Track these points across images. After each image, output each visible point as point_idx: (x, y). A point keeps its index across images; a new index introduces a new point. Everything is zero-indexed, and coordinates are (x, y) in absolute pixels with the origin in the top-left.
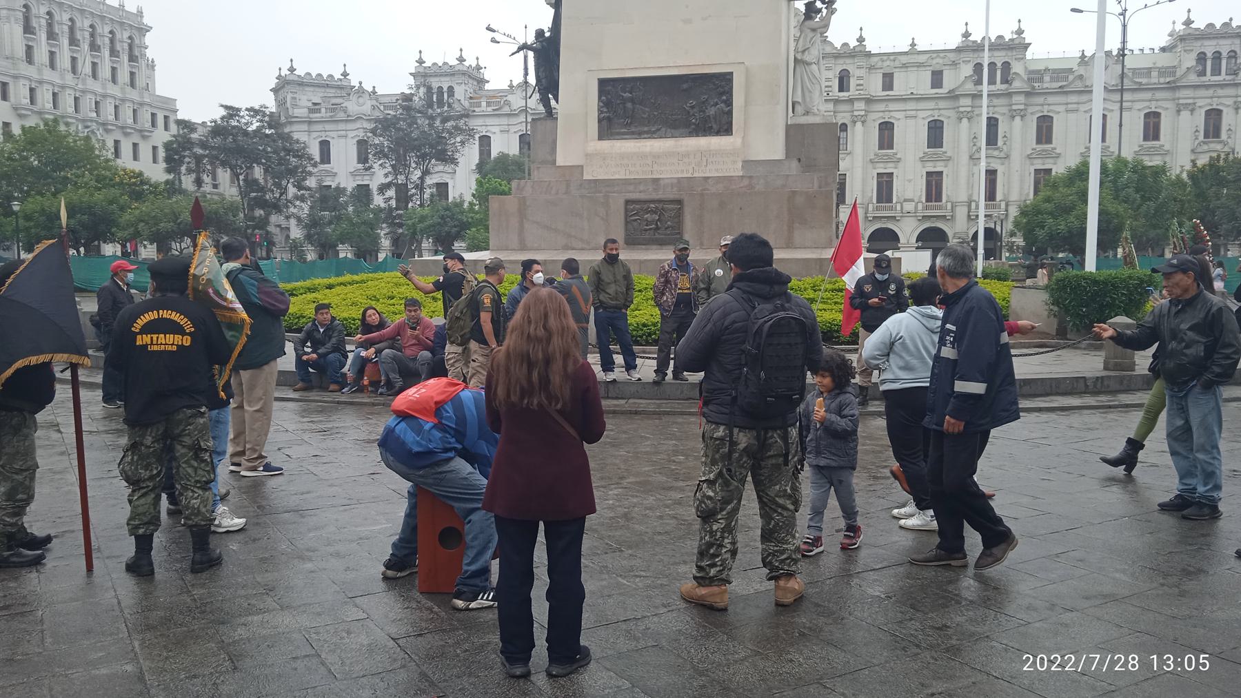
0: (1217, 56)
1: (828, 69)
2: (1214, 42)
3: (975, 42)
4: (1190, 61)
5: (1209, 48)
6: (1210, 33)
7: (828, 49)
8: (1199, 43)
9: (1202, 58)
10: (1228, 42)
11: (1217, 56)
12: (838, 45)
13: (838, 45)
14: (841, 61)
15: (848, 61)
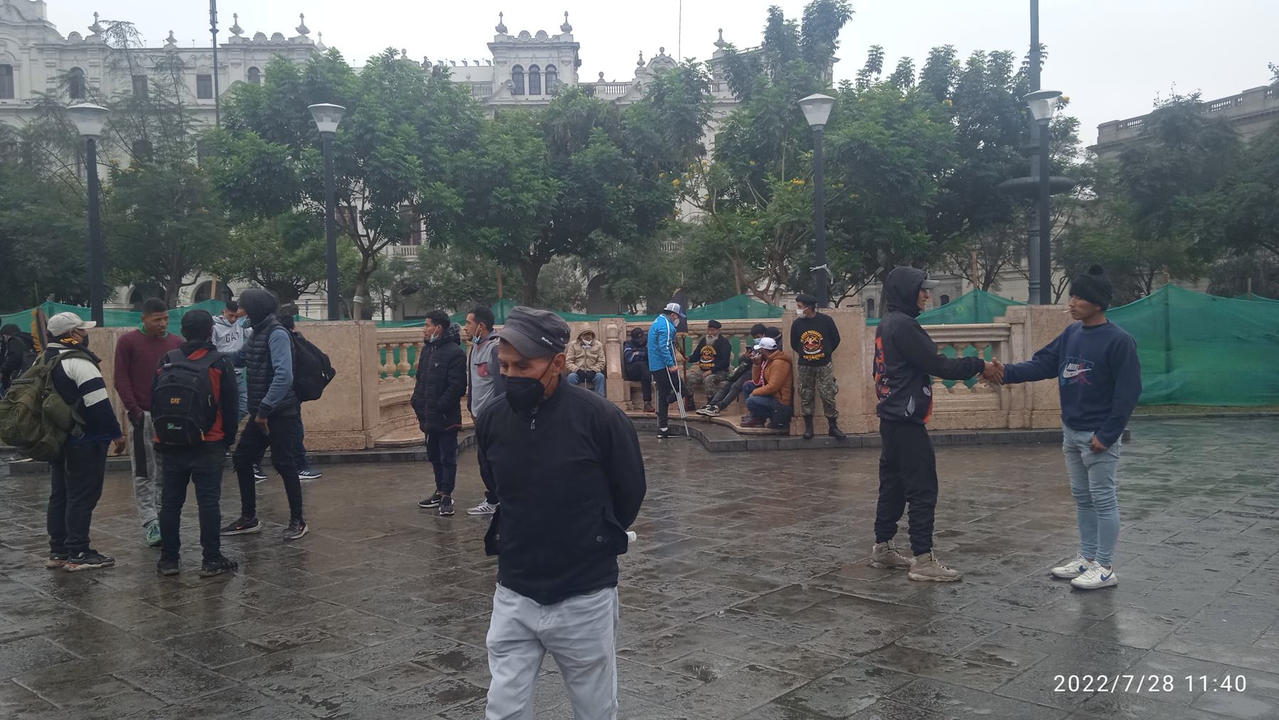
0: (534, 71)
1: (49, 66)
2: (530, 54)
3: (246, 39)
4: (504, 75)
5: (525, 60)
6: (525, 43)
7: (51, 39)
8: (513, 54)
9: (517, 71)
10: (546, 54)
11: (534, 71)
12: (65, 35)
13: (65, 35)
14: (71, 56)
15: (80, 56)
